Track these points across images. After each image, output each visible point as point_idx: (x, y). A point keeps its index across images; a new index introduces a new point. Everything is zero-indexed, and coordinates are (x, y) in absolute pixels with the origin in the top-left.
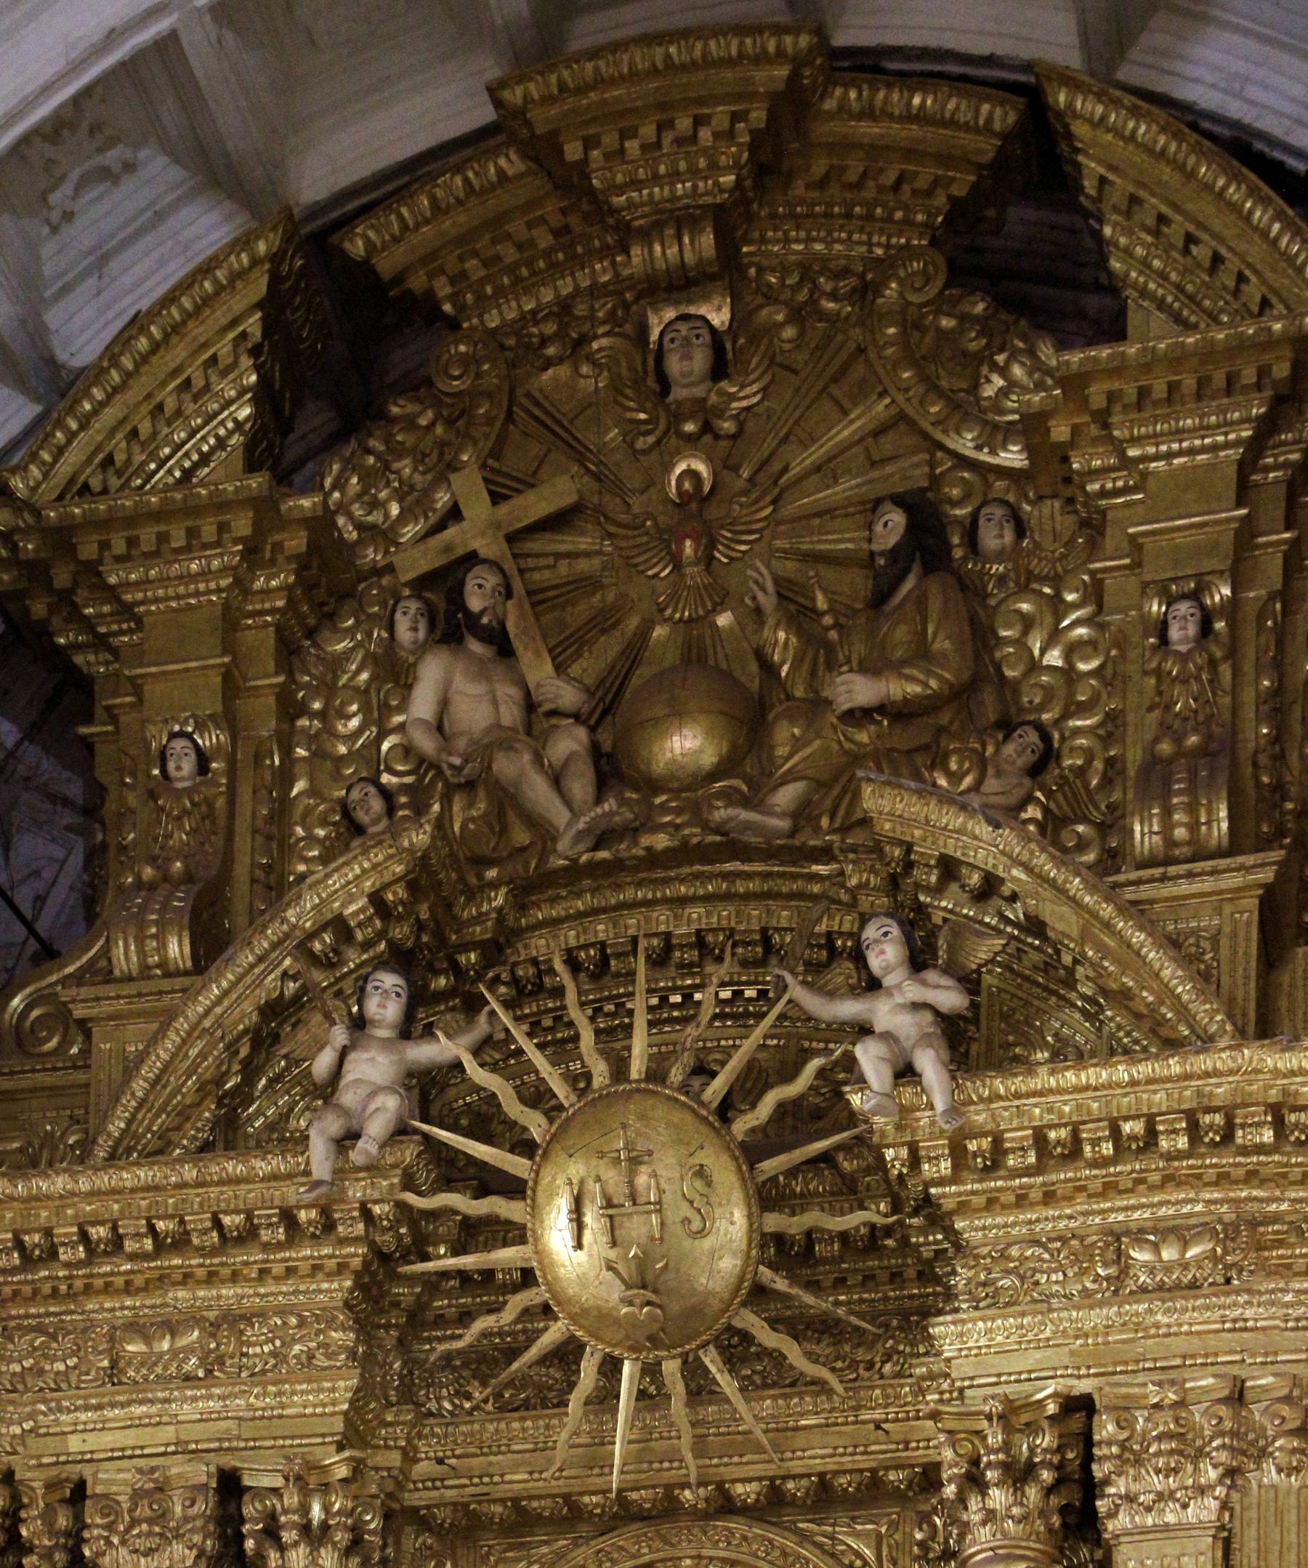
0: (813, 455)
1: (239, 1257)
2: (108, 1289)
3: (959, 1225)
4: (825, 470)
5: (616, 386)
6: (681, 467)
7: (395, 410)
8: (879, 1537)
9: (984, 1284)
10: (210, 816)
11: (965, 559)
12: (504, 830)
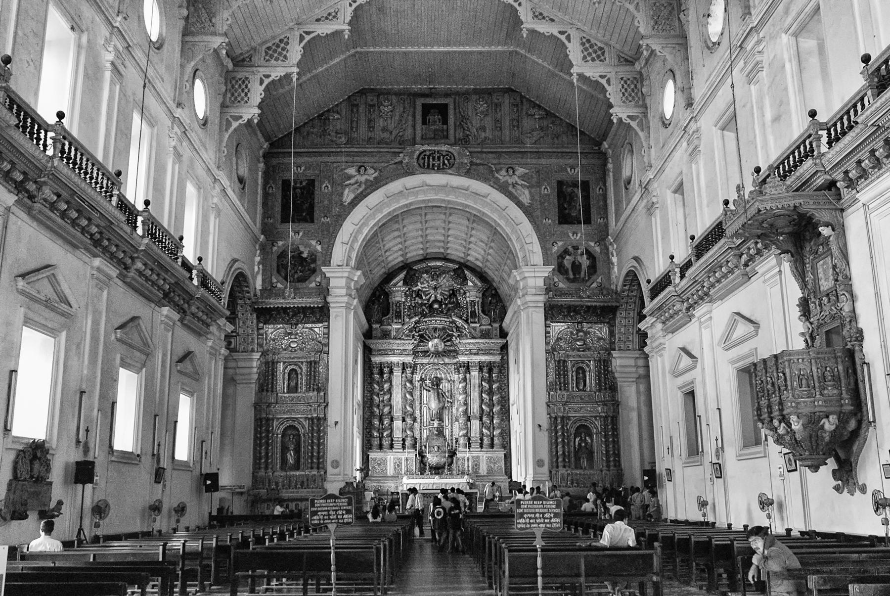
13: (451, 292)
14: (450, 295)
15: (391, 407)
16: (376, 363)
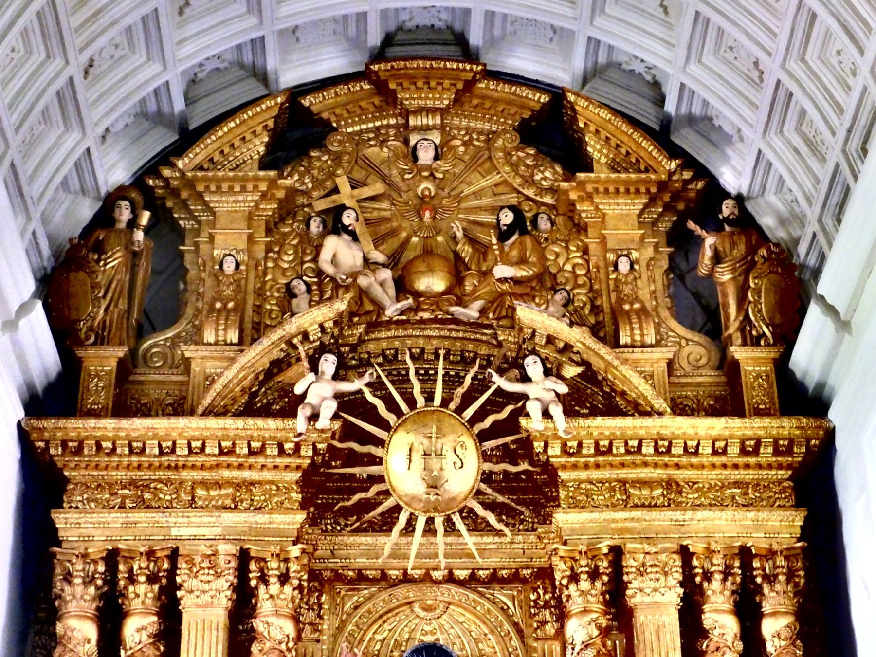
0: (473, 189)
1: (251, 460)
2: (193, 467)
3: (560, 474)
4: (477, 194)
5: (397, 156)
7: (313, 154)
9: (572, 498)
10: (239, 286)
11: (532, 230)
12: (362, 303)
13: (507, 218)
14: (503, 237)
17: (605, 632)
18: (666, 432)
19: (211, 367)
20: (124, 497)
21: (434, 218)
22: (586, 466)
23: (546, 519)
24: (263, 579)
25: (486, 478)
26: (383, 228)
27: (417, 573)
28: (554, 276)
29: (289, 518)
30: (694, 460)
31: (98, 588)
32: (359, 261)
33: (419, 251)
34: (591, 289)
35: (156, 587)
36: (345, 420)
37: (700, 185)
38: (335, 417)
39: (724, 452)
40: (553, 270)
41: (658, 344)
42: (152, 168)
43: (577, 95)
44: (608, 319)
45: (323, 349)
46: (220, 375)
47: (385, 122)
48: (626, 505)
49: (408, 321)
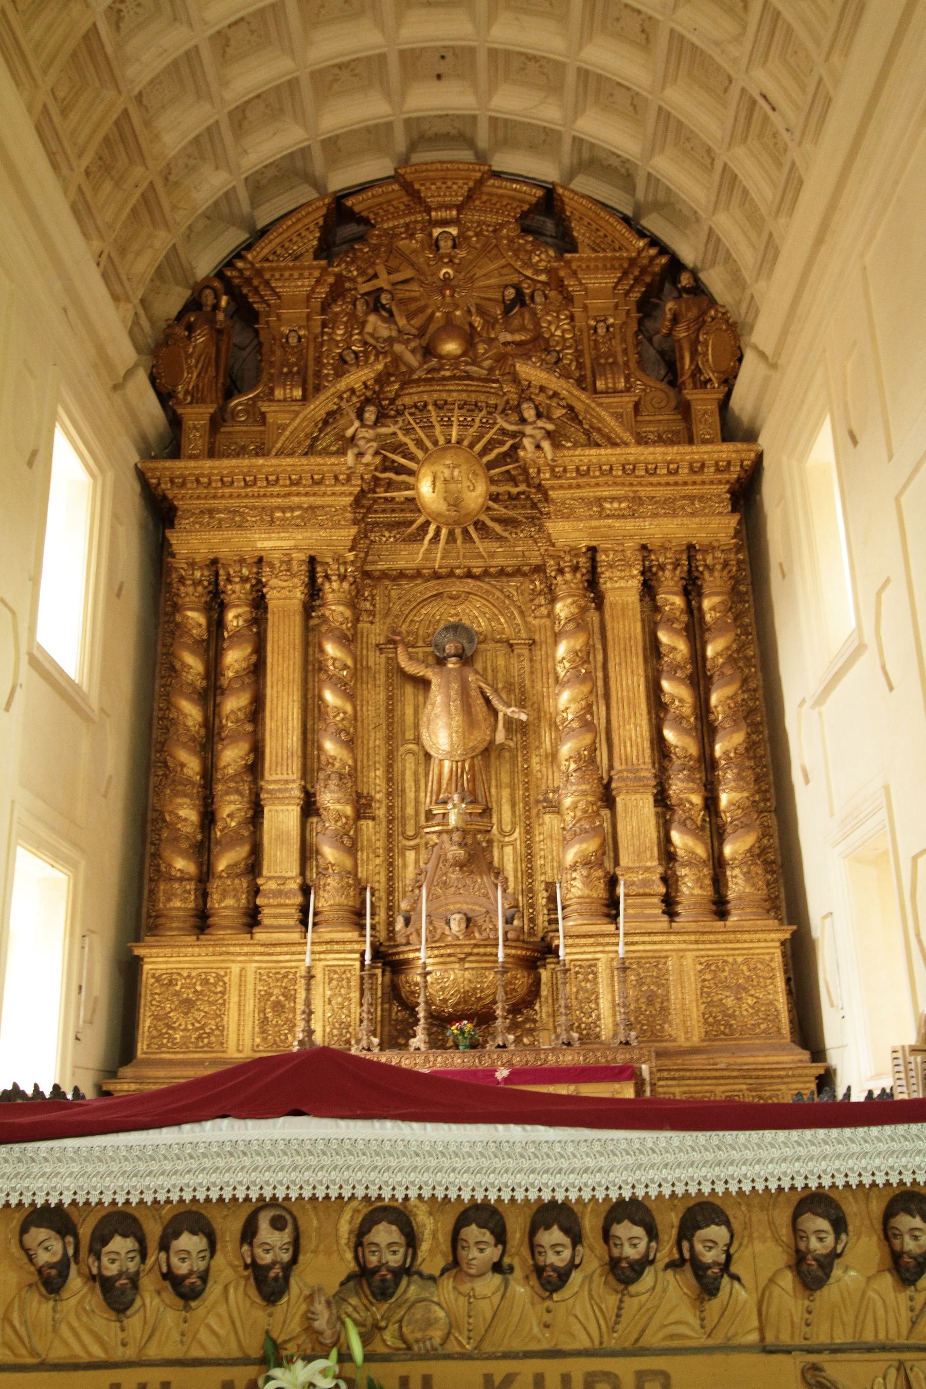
0: (484, 271)
1: (316, 489)
3: (550, 493)
5: (423, 248)
6: (444, 271)
8: (517, 588)
12: (397, 367)
13: (510, 293)
14: (507, 310)
15: (257, 750)
16: (192, 565)
17: (583, 610)
18: (631, 458)
19: (283, 419)
20: (221, 520)
21: (452, 296)
22: (570, 487)
23: (541, 528)
24: (327, 577)
25: (495, 498)
26: (413, 306)
27: (443, 571)
28: (547, 341)
29: (344, 532)
30: (654, 480)
31: (205, 588)
32: (394, 334)
33: (442, 323)
34: (576, 350)
35: (248, 586)
36: (385, 457)
37: (664, 260)
38: (377, 453)
39: (677, 472)
40: (547, 336)
41: (628, 390)
42: (229, 263)
43: (565, 188)
44: (589, 373)
45: (368, 401)
46: (288, 425)
47: (413, 218)
48: (602, 515)
49: (433, 379)
